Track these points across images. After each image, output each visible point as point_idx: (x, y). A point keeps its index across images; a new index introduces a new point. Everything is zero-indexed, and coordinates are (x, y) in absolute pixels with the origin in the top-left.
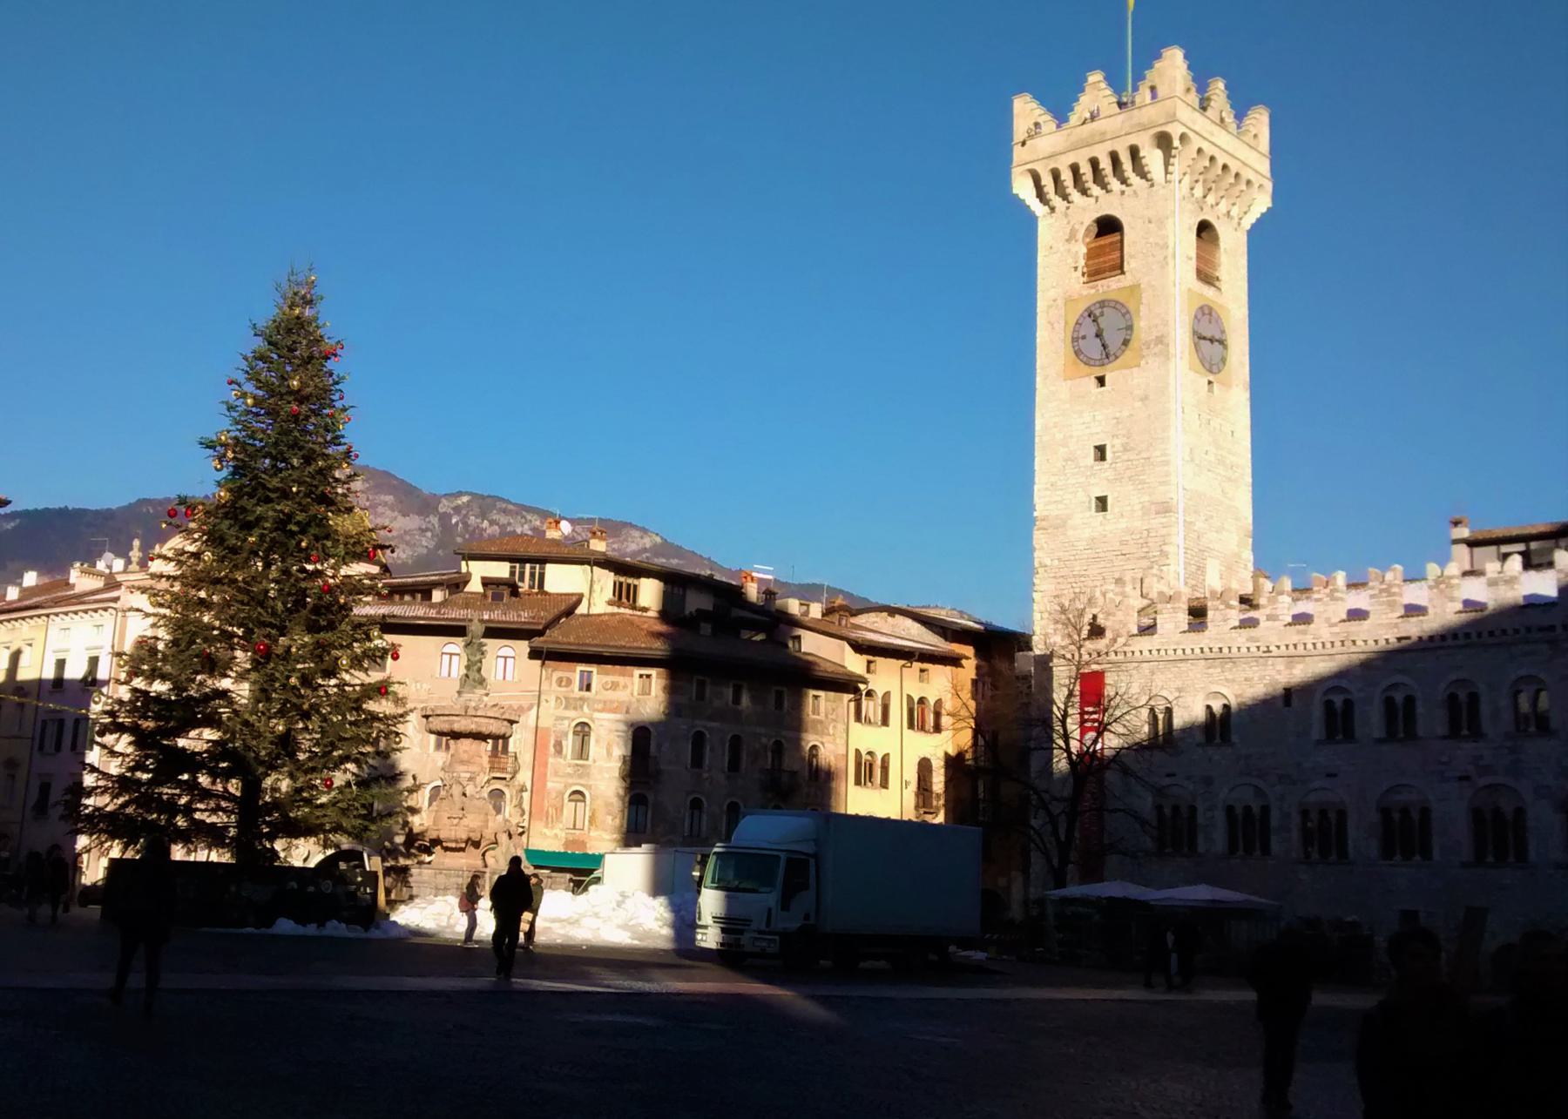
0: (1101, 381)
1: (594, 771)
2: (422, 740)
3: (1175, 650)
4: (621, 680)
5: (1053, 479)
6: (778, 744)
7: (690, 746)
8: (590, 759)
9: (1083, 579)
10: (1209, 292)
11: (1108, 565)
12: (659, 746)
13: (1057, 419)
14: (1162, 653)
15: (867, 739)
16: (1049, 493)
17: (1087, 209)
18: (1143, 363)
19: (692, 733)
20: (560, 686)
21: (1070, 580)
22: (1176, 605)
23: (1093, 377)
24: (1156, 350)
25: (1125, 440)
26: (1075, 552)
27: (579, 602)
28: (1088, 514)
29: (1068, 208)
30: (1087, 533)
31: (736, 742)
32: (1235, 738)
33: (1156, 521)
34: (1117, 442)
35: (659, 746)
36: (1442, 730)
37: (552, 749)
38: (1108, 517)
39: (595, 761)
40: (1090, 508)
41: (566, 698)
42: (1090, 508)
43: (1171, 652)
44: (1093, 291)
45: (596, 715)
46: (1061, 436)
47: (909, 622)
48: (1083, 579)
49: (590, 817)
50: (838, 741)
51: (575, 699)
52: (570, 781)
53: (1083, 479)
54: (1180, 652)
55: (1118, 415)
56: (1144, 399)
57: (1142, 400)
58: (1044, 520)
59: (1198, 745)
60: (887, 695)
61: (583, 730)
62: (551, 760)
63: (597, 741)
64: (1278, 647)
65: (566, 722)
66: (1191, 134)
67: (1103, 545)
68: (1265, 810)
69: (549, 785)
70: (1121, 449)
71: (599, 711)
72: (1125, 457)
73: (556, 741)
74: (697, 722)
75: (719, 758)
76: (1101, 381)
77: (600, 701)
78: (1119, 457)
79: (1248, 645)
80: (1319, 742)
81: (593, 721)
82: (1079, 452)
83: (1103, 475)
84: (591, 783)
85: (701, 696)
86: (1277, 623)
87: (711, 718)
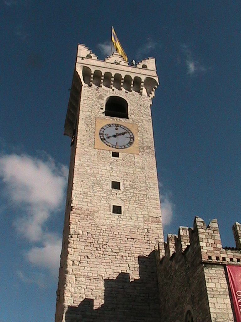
5: (86, 190)
9: (104, 246)
11: (123, 242)
16: (83, 196)
21: (95, 246)
24: (147, 151)
25: (131, 183)
26: (99, 231)
28: (108, 213)
30: (108, 222)
33: (153, 225)
34: (125, 182)
40: (110, 211)
44: (111, 119)
48: (104, 246)
55: (127, 171)
56: (143, 168)
57: (140, 168)
58: (78, 209)
67: (119, 231)
70: (129, 187)
76: (116, 155)
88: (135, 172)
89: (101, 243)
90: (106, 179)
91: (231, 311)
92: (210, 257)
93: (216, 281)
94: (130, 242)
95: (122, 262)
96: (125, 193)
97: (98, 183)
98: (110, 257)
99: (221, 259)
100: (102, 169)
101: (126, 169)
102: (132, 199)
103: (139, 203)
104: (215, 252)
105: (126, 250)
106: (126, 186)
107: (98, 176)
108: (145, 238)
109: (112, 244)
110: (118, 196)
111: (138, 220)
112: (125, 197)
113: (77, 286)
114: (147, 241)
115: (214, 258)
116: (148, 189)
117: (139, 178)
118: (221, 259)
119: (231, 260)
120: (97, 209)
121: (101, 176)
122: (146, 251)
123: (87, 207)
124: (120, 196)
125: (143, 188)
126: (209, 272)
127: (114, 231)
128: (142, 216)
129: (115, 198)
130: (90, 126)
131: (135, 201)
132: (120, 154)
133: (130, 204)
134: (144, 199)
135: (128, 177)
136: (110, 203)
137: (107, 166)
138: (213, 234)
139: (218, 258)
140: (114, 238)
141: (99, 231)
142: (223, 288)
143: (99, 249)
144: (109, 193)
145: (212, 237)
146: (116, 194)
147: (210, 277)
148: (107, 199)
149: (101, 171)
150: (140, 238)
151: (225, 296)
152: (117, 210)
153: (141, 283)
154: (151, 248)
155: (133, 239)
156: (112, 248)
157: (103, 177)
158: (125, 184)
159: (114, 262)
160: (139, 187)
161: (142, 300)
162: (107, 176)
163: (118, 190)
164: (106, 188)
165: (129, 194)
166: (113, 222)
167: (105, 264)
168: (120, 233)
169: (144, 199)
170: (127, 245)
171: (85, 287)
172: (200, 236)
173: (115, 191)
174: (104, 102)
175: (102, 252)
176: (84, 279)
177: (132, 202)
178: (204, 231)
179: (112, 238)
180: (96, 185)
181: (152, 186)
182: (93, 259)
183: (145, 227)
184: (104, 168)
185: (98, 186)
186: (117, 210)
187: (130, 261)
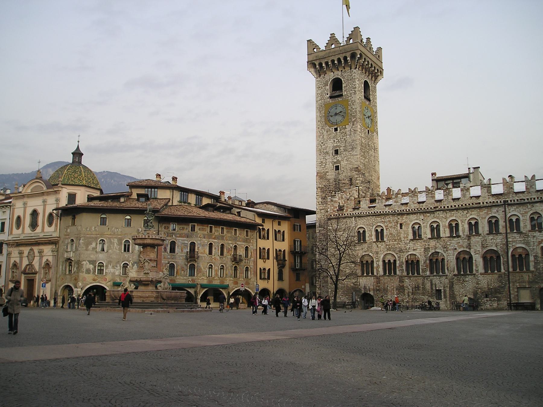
0: (336, 130)
1: (177, 256)
2: (119, 248)
3: (366, 213)
4: (185, 227)
5: (322, 160)
6: (235, 246)
7: (208, 248)
8: (176, 253)
10: (368, 103)
12: (198, 248)
13: (323, 141)
14: (362, 213)
15: (263, 244)
16: (320, 164)
17: (331, 76)
18: (349, 124)
19: (209, 244)
20: (165, 229)
22: (366, 199)
27: (169, 201)
29: (325, 75)
31: (222, 245)
32: (385, 239)
35: (198, 248)
36: (448, 234)
37: (163, 250)
39: (177, 254)
41: (167, 233)
43: (365, 213)
45: (177, 238)
47: (273, 207)
49: (176, 272)
50: (254, 245)
51: (170, 233)
52: (170, 260)
54: (367, 213)
57: (349, 135)
59: (374, 242)
60: (268, 230)
61: (173, 244)
62: (163, 253)
63: (178, 247)
64: (398, 211)
65: (168, 241)
66: (362, 53)
68: (395, 261)
69: (163, 261)
70: (343, 150)
71: (178, 237)
72: (344, 153)
73: (164, 247)
74: (210, 240)
75: (216, 251)
76: (336, 130)
77: (178, 234)
78: (342, 153)
79: (389, 210)
80: (411, 240)
81: (176, 241)
84: (176, 261)
85: (211, 231)
86: (397, 203)
87: (214, 239)
92: (331, 215)
115: (332, 215)
123: (323, 171)
139: (334, 215)
146: (337, 158)
174: (328, 87)
181: (355, 147)
184: (330, 142)
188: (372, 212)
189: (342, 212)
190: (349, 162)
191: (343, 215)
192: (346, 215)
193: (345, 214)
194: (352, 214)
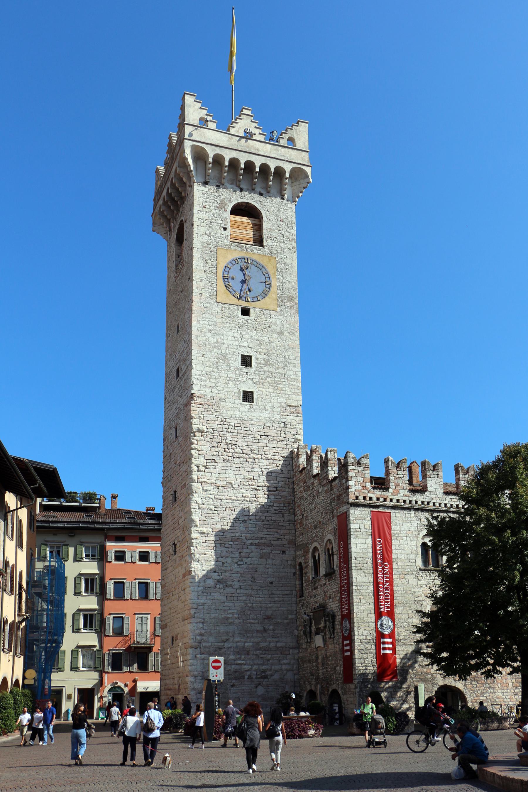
9: (233, 447)
21: (223, 446)
23: (240, 308)
26: (227, 427)
28: (237, 401)
30: (237, 414)
33: (292, 417)
38: (254, 407)
42: (239, 397)
46: (215, 340)
48: (233, 447)
53: (233, 376)
55: (261, 338)
67: (250, 426)
70: (263, 362)
82: (229, 356)
83: (249, 376)
88: (271, 339)
89: (230, 442)
90: (234, 352)
91: (371, 551)
92: (357, 497)
93: (361, 521)
94: (264, 440)
95: (254, 466)
96: (257, 372)
97: (223, 358)
98: (241, 460)
99: (368, 499)
100: (228, 336)
101: (260, 335)
102: (266, 381)
103: (274, 385)
104: (363, 491)
105: (258, 451)
106: (259, 362)
107: (224, 348)
108: (282, 435)
109: (243, 443)
110: (249, 376)
111: (273, 411)
112: (258, 377)
113: (205, 496)
114: (283, 439)
115: (361, 498)
116: (287, 365)
117: (275, 349)
118: (368, 499)
119: (378, 499)
120: (223, 396)
121: (227, 346)
122: (282, 452)
124: (251, 377)
125: (280, 364)
126: (355, 513)
127: (245, 425)
128: (279, 405)
129: (245, 380)
130: (209, 262)
131: (270, 384)
132: (251, 310)
133: (264, 388)
134: (282, 380)
135: (262, 347)
136: (239, 387)
137: (235, 330)
138: (363, 472)
139: (365, 498)
140: (245, 435)
141: (227, 427)
142: (366, 529)
143: (227, 450)
144: (237, 372)
145: (362, 474)
147: (355, 518)
148: (237, 381)
149: (227, 339)
150: (276, 435)
151: (367, 537)
152: (248, 397)
153: (275, 491)
154: (288, 447)
155: (267, 436)
156: (242, 448)
157: (230, 349)
158: (257, 359)
159: (245, 466)
160: (275, 363)
161: (275, 510)
162: (235, 347)
163: (249, 368)
164: (234, 365)
165: (263, 373)
166: (243, 414)
167: (234, 469)
168: (252, 429)
169: (282, 380)
170: (260, 444)
171: (213, 496)
172: (350, 474)
173: (245, 369)
175: (230, 454)
176: (212, 488)
177: (267, 385)
178: (354, 467)
179: (243, 435)
180: (221, 361)
182: (220, 463)
183: (282, 420)
184: (231, 334)
185: (223, 362)
186: (248, 397)
187: (263, 464)
188: (452, 505)
189: (385, 493)
190: (278, 392)
191: (388, 500)
192: (395, 501)
193: (391, 500)
194: (408, 502)
